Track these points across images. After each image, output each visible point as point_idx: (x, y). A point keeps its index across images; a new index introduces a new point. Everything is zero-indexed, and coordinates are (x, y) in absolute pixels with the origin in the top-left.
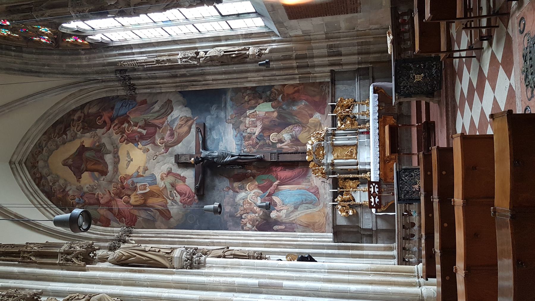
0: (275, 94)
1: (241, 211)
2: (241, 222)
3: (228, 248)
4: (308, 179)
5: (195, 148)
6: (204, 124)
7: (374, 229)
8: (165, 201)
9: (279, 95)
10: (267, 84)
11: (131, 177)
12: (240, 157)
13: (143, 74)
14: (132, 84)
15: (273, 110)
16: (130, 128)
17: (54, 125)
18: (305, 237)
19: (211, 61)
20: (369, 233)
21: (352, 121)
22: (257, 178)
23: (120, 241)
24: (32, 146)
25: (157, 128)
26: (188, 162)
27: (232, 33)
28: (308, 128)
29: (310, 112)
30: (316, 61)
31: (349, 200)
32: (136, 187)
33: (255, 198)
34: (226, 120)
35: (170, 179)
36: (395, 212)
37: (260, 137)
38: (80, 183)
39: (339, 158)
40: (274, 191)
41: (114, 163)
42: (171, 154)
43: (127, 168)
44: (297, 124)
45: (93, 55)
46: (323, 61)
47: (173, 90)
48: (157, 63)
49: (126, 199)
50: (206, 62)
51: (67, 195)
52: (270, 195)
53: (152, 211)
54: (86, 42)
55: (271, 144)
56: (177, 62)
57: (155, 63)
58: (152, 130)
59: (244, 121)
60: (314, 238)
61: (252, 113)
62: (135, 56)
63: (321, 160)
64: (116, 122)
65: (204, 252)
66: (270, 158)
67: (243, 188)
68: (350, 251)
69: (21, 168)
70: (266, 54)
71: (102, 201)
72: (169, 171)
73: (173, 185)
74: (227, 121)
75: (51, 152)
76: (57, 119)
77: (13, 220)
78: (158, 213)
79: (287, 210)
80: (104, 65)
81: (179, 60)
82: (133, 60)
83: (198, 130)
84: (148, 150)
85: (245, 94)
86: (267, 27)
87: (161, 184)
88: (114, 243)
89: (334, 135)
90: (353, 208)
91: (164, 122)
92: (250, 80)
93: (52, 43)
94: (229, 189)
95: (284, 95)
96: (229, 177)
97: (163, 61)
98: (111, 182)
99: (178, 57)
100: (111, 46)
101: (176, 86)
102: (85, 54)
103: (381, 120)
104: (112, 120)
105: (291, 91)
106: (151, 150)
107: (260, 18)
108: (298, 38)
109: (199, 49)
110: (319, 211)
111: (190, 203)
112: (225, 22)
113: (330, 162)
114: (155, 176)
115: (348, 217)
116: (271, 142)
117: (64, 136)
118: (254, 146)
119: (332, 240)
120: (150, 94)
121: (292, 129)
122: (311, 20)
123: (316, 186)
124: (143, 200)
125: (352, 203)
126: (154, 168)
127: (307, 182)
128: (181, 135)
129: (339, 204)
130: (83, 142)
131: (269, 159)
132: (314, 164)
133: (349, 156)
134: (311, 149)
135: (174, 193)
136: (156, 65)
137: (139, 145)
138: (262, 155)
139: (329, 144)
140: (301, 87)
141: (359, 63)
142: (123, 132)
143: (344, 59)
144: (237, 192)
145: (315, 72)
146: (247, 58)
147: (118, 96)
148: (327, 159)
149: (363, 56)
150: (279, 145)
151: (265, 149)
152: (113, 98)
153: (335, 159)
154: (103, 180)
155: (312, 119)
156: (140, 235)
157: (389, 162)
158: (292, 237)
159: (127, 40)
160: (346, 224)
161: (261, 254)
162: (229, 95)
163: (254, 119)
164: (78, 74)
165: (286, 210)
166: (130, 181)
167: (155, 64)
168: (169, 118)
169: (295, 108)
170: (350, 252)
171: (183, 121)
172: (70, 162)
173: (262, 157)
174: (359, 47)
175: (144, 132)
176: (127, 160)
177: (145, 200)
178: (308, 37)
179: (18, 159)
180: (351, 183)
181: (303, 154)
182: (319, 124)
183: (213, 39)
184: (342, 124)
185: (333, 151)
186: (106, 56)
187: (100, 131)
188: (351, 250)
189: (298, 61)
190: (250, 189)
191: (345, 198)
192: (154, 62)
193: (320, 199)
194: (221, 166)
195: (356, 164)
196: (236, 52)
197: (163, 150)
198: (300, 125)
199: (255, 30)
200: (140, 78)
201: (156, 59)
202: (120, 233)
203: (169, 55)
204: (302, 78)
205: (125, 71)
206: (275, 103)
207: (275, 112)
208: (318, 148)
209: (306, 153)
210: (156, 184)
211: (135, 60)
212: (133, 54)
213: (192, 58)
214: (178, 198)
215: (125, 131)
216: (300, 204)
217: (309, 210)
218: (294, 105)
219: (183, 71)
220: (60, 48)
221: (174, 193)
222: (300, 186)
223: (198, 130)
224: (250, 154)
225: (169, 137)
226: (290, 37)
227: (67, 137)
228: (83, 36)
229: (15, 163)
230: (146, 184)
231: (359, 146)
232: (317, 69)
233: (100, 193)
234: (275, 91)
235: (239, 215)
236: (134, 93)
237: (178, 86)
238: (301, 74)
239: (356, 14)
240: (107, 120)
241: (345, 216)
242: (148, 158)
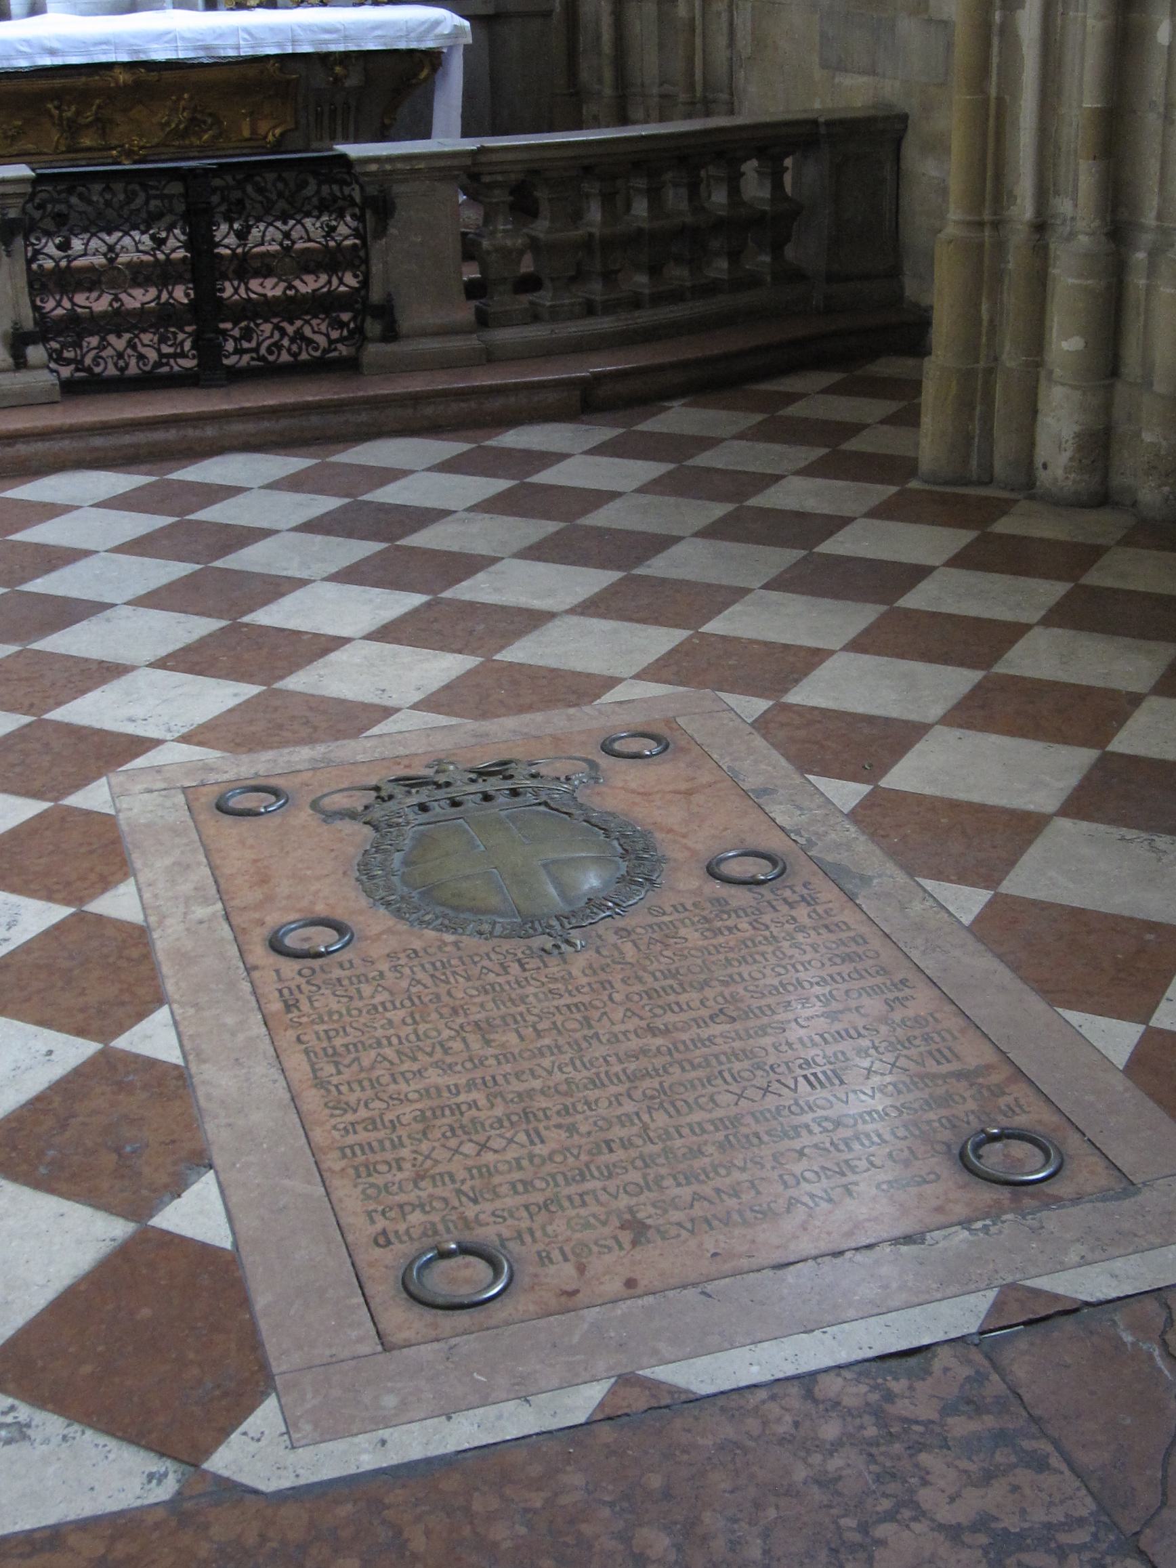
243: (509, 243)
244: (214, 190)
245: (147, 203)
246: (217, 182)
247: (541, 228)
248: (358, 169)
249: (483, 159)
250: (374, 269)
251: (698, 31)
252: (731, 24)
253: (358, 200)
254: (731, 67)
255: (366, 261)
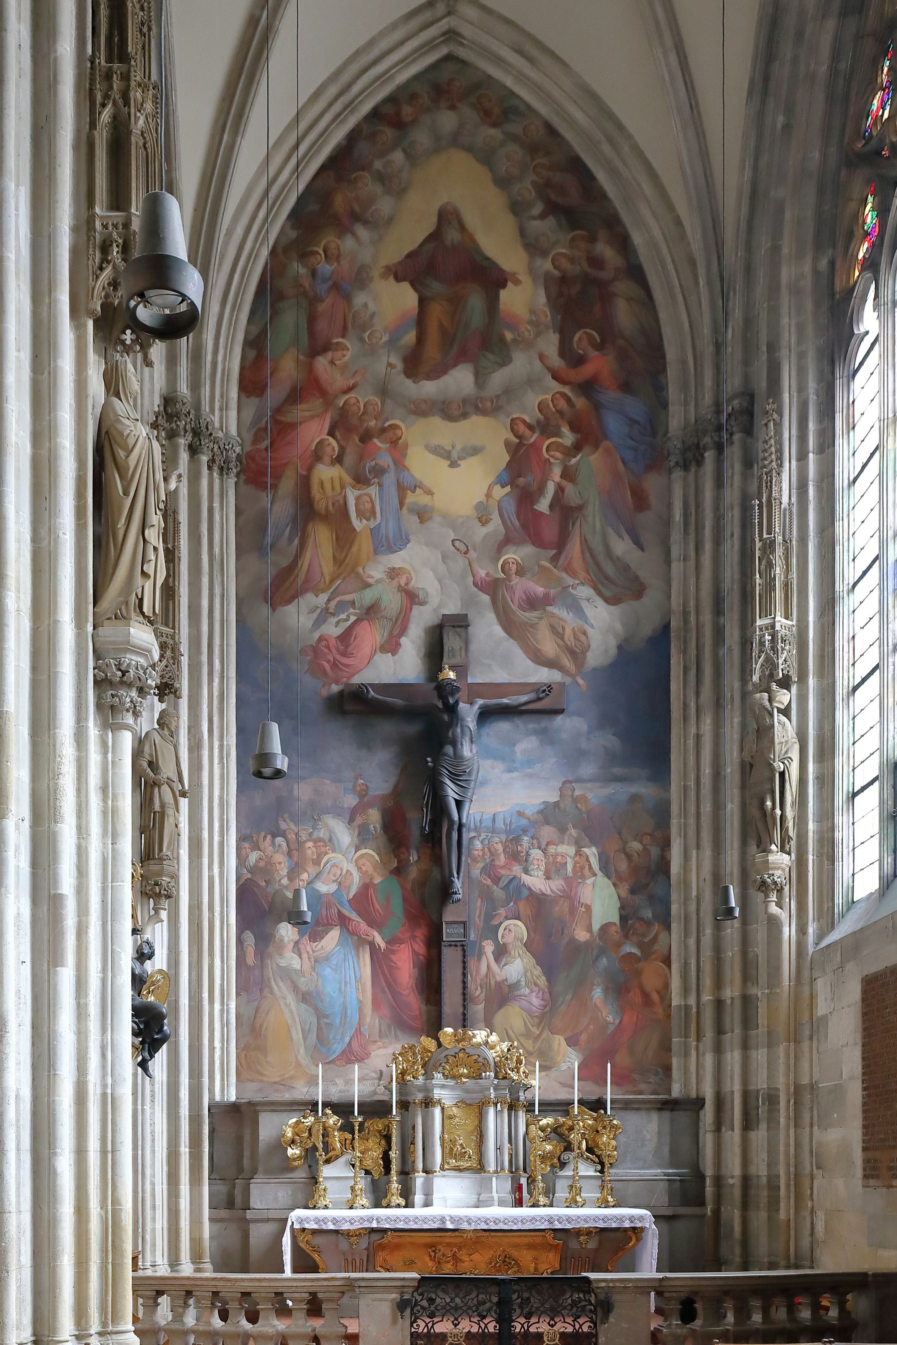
0: (643, 935)
1: (297, 834)
2: (263, 834)
3: (183, 794)
4: (390, 1031)
5: (487, 681)
6: (560, 711)
7: (249, 1215)
8: (322, 586)
9: (640, 946)
10: (674, 908)
11: (400, 464)
12: (456, 827)
13: (731, 496)
14: (702, 456)
15: (596, 927)
16: (558, 455)
17: (577, 166)
18: (225, 1024)
19: (758, 731)
20: (238, 1200)
21: (551, 1158)
22: (394, 881)
23: (196, 433)
24: (509, 82)
25: (554, 552)
26: (445, 660)
27: (840, 798)
28: (538, 1033)
29: (583, 1037)
30: (733, 1058)
31: (327, 1148)
32: (366, 482)
33: (335, 875)
34: (571, 782)
35: (391, 601)
36: (295, 1271)
37: (515, 889)
38: (385, 275)
39: (447, 1122)
40: (353, 933)
41: (444, 402)
42: (468, 601)
43: (428, 448)
44: (551, 1001)
45: (809, 305)
46: (732, 1078)
47: (676, 602)
48: (764, 544)
49: (328, 450)
50: (755, 713)
51: (343, 230)
52: (343, 921)
53: (290, 540)
54: (857, 273)
55: (495, 922)
56: (763, 614)
57: (765, 536)
58: (550, 531)
59: (566, 838)
60: (222, 1049)
61: (590, 865)
62: (794, 463)
63: (440, 1069)
64: (580, 402)
65: (166, 720)
66: (451, 920)
67: (363, 837)
68: (187, 1150)
69: (434, 39)
70: (766, 907)
71: (321, 363)
72: (417, 596)
73: (371, 611)
74: (568, 785)
75: (486, 157)
76: (601, 176)
77: (252, 21)
78: (285, 562)
79: (301, 972)
80: (773, 347)
81: (766, 621)
82: (780, 459)
83: (544, 691)
84: (484, 519)
85: (647, 840)
86: (848, 910)
87: (375, 572)
88: (189, 413)
89: (512, 1107)
90: (306, 1157)
91: (573, 574)
92: (691, 857)
93: (864, 137)
94: (362, 794)
95: (639, 960)
96: (396, 793)
97: (770, 565)
98: (384, 391)
99: (778, 618)
100: (833, 373)
101: (685, 614)
102: (816, 272)
103: (549, 1236)
104: (587, 388)
105: (651, 981)
106: (484, 530)
107: (877, 887)
108: (805, 1004)
109: (799, 690)
110: (298, 1064)
111: (316, 670)
112: (876, 773)
113: (436, 1097)
114: (401, 549)
115: (279, 1146)
116: (501, 923)
117: (538, 208)
118: (490, 870)
119: (218, 1098)
120: (667, 522)
121: (535, 984)
122: (855, 1044)
123: (368, 1055)
124: (327, 507)
125: (321, 1156)
126: (426, 544)
127: (380, 1030)
128: (529, 632)
129: (317, 1119)
130: (517, 282)
131: (447, 917)
132: (430, 1051)
133: (452, 1149)
134: (474, 1040)
135: (348, 616)
136: (757, 540)
137: (503, 487)
138: (460, 896)
139: (487, 1093)
140: (660, 1011)
141: (718, 1180)
142: (546, 428)
143: (733, 1137)
144: (351, 820)
145: (701, 1052)
146: (758, 847)
147: (665, 405)
148: (443, 1087)
149: (737, 1193)
150: (489, 948)
151: (479, 903)
152: (659, 389)
153: (443, 1109)
154: (390, 365)
155: (563, 1043)
156: (216, 505)
157: (430, 1256)
158: (222, 985)
159: (851, 433)
160: (261, 1138)
161: (168, 897)
162: (646, 790)
163: (570, 867)
164: (749, 248)
165: (299, 967)
166: (385, 460)
167: (761, 535)
168: (584, 592)
169: (598, 994)
170: (184, 1149)
171: (572, 639)
172: (452, 236)
173: (456, 897)
174: (764, 1180)
175: (543, 505)
176: (453, 447)
177: (325, 518)
178: (807, 1033)
179: (466, 30)
180: (376, 1153)
181: (461, 1017)
182: (547, 1063)
183: (827, 734)
184: (542, 1129)
185: (466, 1104)
186: (801, 356)
187: (550, 344)
188: (190, 1152)
189: (738, 1003)
190: (361, 862)
191: (334, 1136)
192: (769, 533)
193: (332, 1066)
194: (428, 767)
195: (429, 1167)
196: (778, 812)
197: (483, 573)
198: (548, 1008)
199: (843, 870)
200: (719, 484)
201: (779, 539)
202: (220, 434)
203: (787, 586)
204: (685, 1014)
205: (749, 431)
206: (615, 933)
207: (588, 935)
208: (476, 1061)
209: (464, 1026)
210: (376, 552)
211: (780, 465)
212: (802, 457)
213: (771, 664)
214: (332, 629)
215: (548, 438)
216: (316, 1009)
217: (301, 1036)
218: (606, 991)
219: (732, 635)
220: (844, 172)
221: (348, 616)
222: (368, 1009)
223: (546, 690)
224: (463, 858)
225: (525, 593)
226: (813, 980)
227: (534, 218)
228: (878, 265)
229: (449, 14)
230: (375, 518)
231: (478, 1176)
232: (709, 1060)
233: (349, 355)
234: (652, 935)
235: (283, 826)
236: (672, 464)
237: (686, 621)
238: (698, 1013)
239: (859, 1172)
240: (588, 370)
241: (283, 1136)
242: (460, 520)
243: (679, 1331)
244: (515, 1292)
245: (477, 1296)
246: (516, 1287)
247: (698, 1324)
248: (594, 1285)
249: (664, 1284)
250: (600, 1341)
251: (792, 1225)
252: (812, 1223)
253: (593, 1302)
254: (812, 1247)
255: (596, 1336)
